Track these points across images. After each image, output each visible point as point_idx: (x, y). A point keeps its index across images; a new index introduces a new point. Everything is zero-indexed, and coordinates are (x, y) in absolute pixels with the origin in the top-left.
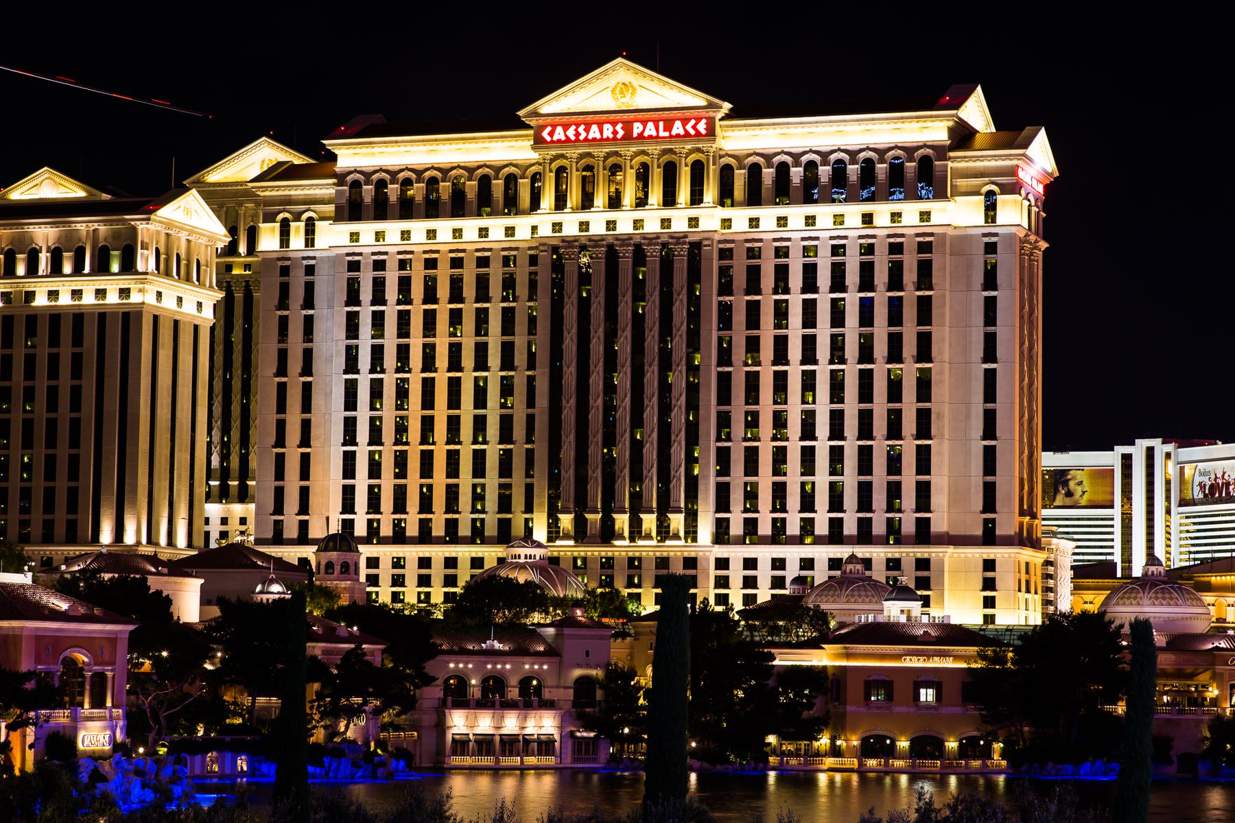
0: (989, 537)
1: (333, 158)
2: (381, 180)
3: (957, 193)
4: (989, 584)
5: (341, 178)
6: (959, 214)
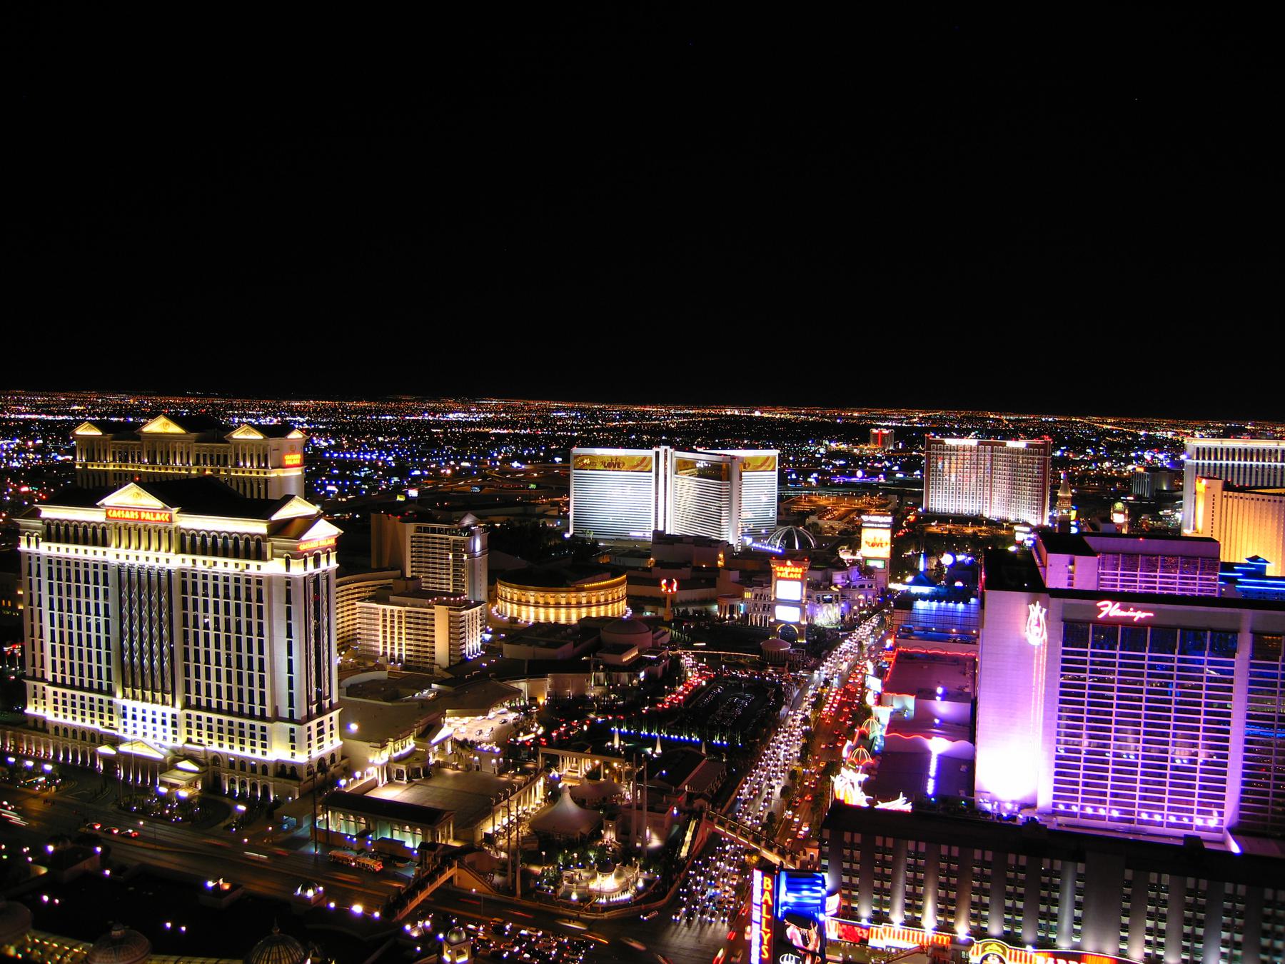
0: (291, 719)
1: (39, 512)
2: (59, 523)
3: (273, 556)
4: (292, 739)
5: (43, 520)
6: (273, 567)
